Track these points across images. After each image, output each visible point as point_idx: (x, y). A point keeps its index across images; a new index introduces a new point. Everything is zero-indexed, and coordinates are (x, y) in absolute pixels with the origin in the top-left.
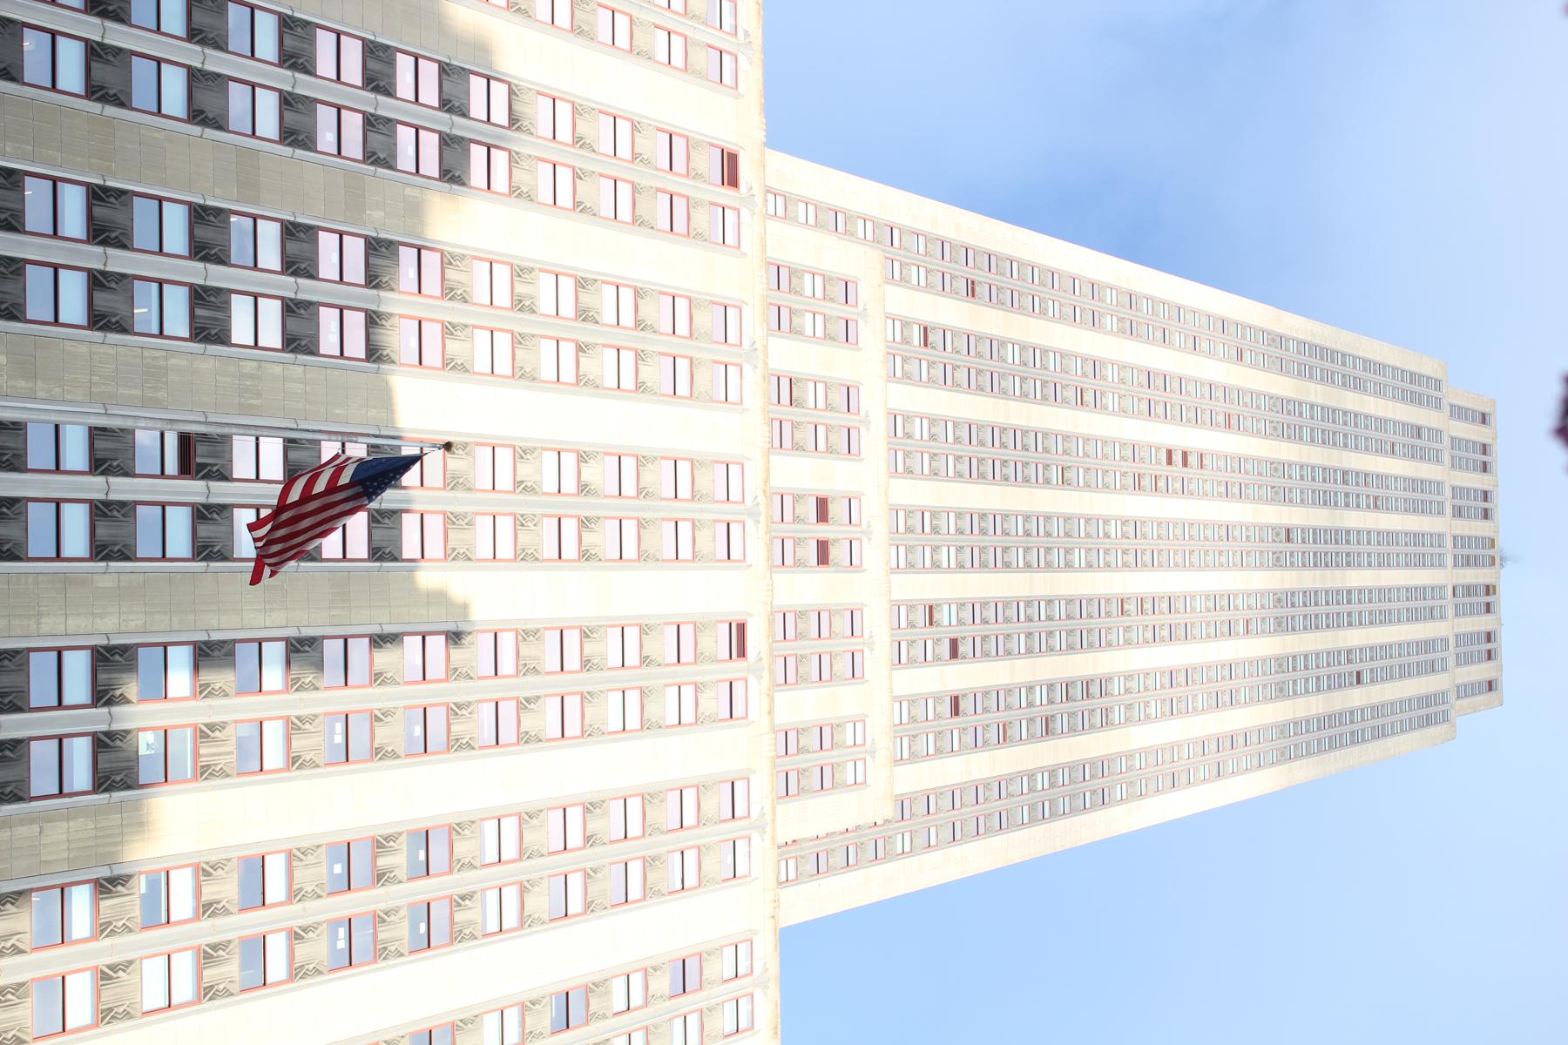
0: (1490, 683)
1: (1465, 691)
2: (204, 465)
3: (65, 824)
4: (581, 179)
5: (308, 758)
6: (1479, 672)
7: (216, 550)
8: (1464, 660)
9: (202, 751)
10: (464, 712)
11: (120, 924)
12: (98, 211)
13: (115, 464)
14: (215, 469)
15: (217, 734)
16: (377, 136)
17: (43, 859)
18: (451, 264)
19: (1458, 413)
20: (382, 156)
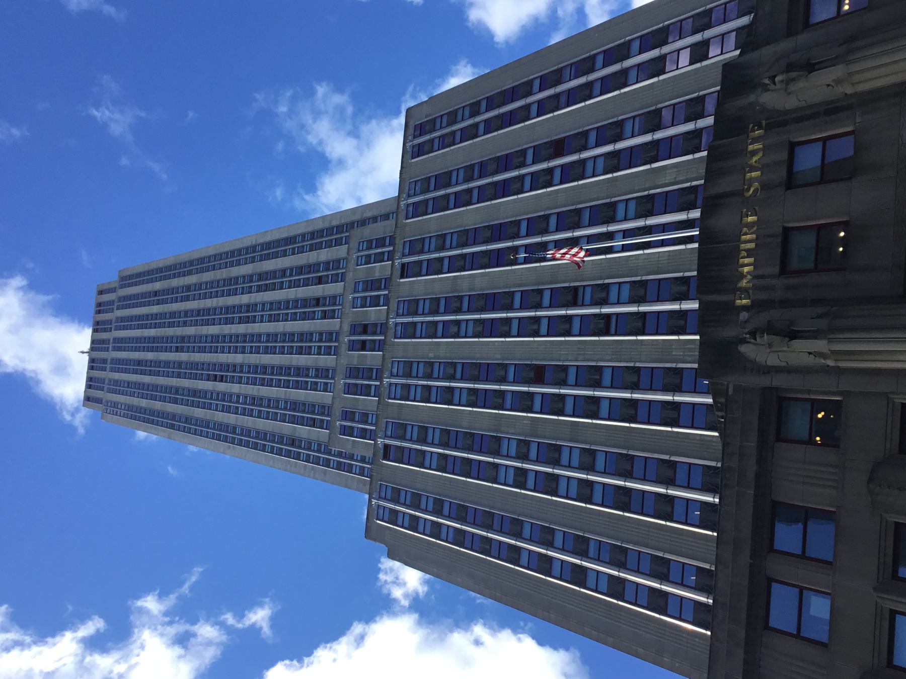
0: (101, 294)
1: (112, 290)
2: (600, 320)
3: (667, 182)
4: (446, 443)
5: (573, 213)
6: (106, 298)
7: (600, 288)
8: (111, 303)
9: (612, 213)
10: (512, 235)
11: (650, 146)
12: (633, 412)
13: (635, 317)
14: (597, 318)
15: (606, 219)
16: (523, 451)
17: (675, 170)
18: (500, 405)
19: (98, 401)
20: (523, 444)
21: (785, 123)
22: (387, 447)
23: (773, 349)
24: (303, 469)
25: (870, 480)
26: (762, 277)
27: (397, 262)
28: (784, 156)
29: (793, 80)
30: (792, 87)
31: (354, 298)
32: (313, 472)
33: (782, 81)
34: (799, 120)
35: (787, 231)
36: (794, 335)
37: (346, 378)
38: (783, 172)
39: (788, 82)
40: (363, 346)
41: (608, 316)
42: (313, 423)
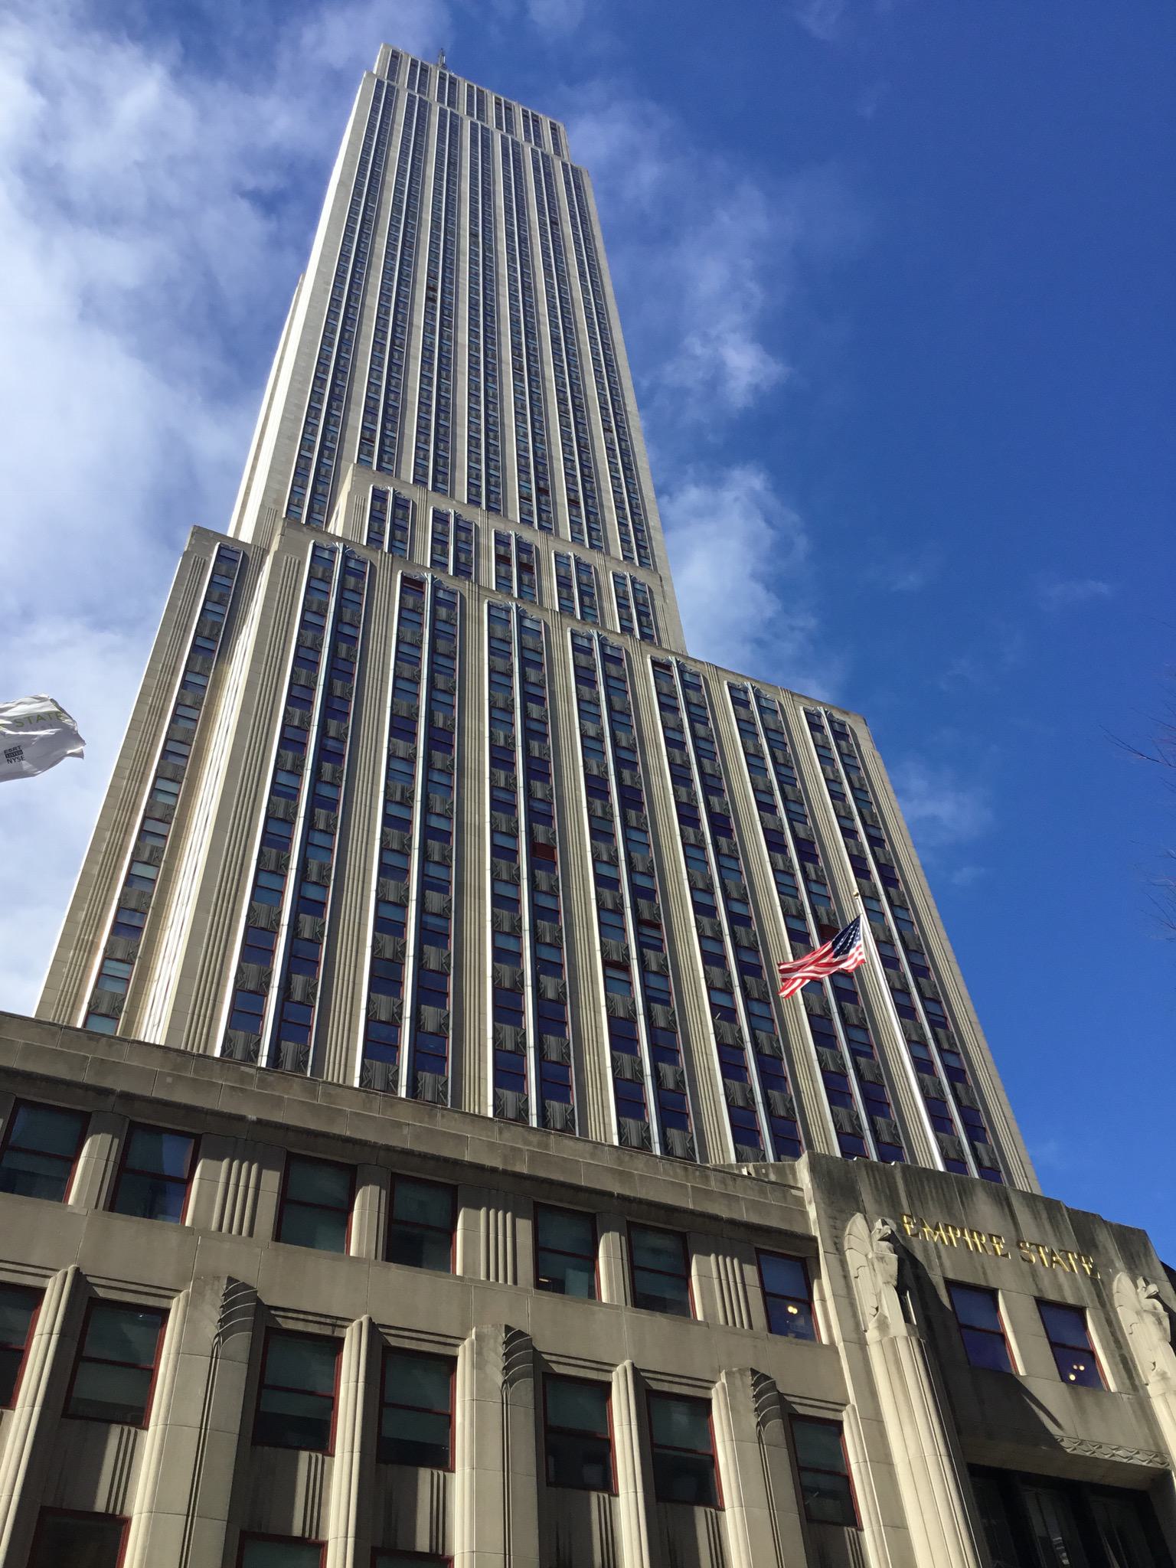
21: (1103, 1304)
22: (421, 584)
23: (876, 1263)
24: (296, 402)
25: (754, 1372)
26: (939, 1257)
27: (672, 659)
28: (1071, 1300)
29: (1160, 1323)
30: (1149, 1320)
31: (568, 558)
32: (293, 417)
33: (1155, 1308)
34: (1109, 1322)
35: (992, 1294)
36: (900, 1290)
37: (457, 520)
38: (1052, 1295)
39: (1155, 1314)
40: (502, 560)
41: (626, 968)
42: (366, 441)
